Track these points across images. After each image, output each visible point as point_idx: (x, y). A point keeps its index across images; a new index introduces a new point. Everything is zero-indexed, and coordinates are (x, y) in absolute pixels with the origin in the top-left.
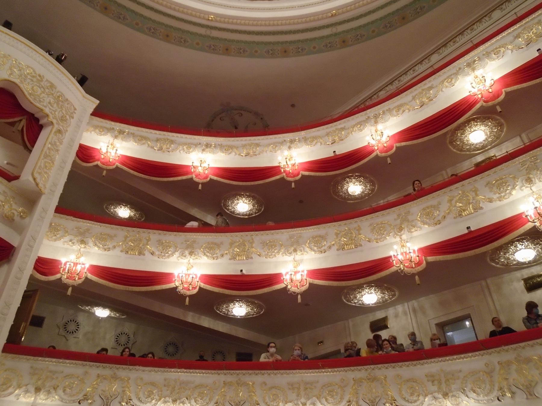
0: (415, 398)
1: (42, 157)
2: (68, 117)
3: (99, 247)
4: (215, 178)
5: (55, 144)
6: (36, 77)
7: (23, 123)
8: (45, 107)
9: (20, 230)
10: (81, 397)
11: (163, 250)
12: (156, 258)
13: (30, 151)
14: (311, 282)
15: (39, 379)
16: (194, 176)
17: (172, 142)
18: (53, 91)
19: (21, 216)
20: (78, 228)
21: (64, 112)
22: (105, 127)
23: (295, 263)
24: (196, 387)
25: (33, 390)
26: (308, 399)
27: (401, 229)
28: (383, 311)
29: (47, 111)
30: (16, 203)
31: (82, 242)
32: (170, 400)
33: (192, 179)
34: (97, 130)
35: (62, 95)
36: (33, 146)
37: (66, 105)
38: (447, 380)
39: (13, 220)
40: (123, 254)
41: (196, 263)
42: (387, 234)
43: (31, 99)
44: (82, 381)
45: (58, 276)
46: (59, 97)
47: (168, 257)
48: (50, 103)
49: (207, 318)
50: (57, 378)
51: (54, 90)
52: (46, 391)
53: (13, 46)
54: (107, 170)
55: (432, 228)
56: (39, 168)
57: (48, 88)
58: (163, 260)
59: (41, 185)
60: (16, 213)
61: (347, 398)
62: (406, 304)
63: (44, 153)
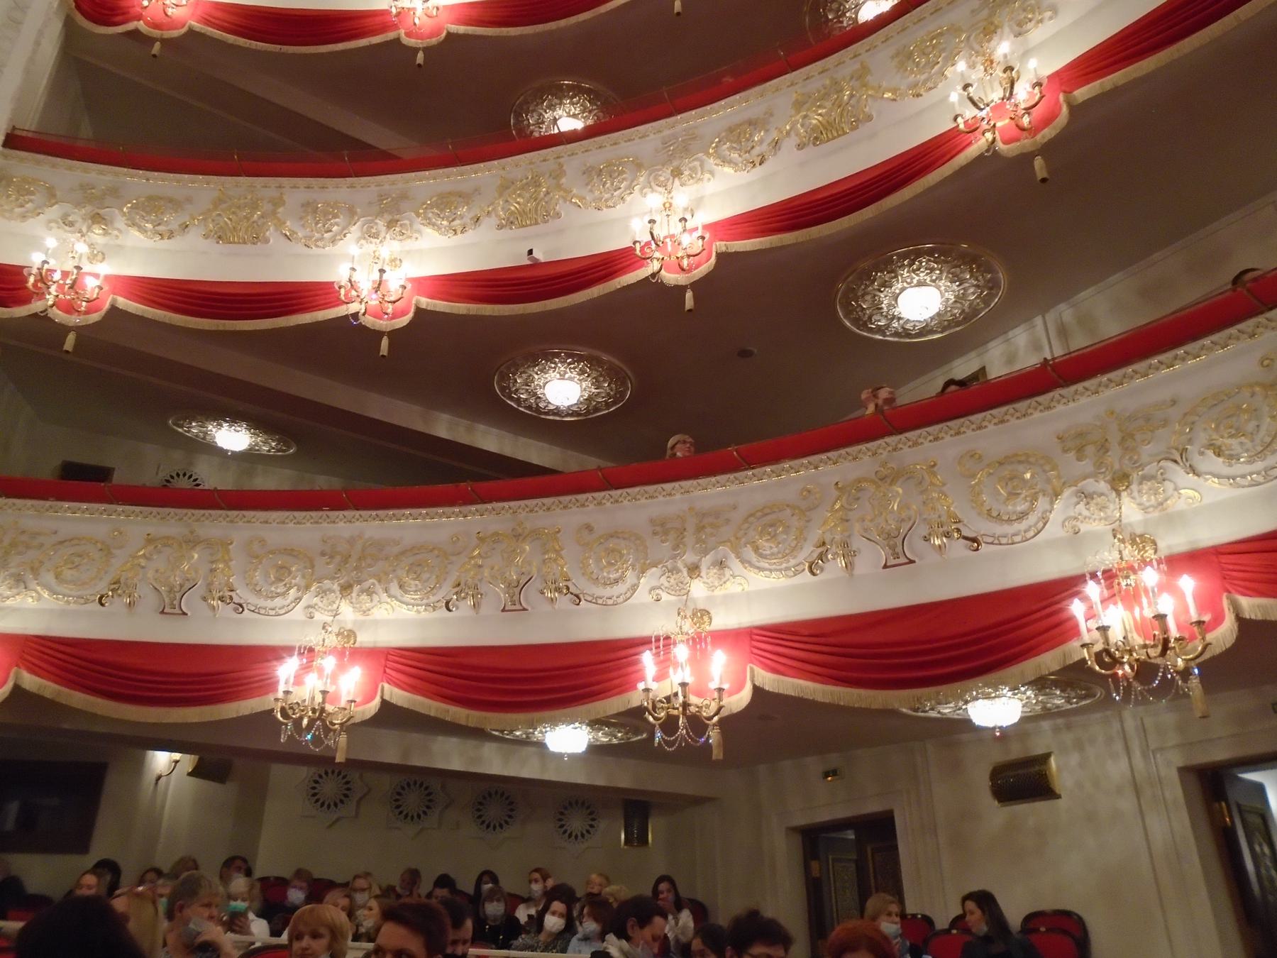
0: (1021, 507)
3: (142, 230)
4: (462, 29)
10: (102, 586)
11: (317, 223)
14: (724, 249)
16: (402, 32)
20: (83, 187)
24: (403, 553)
26: (705, 552)
27: (990, 31)
28: (973, 354)
31: (97, 219)
32: (336, 587)
38: (1127, 438)
40: (210, 246)
41: (409, 252)
44: (107, 550)
47: (333, 241)
49: (494, 430)
50: (42, 545)
52: (12, 575)
54: (164, 42)
58: (320, 251)
61: (816, 534)
62: (1038, 320)
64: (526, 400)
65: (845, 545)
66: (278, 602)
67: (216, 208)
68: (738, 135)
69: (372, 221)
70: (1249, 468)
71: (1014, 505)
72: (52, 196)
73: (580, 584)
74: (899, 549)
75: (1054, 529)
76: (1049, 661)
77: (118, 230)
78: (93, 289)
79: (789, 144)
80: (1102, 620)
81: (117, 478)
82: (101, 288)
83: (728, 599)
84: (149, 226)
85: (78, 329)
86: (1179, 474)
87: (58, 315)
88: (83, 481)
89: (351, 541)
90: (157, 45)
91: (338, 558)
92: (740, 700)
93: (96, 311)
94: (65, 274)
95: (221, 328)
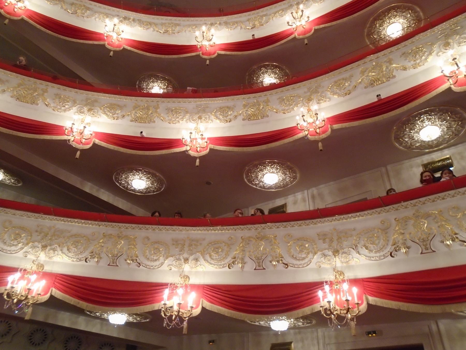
0: (304, 256)
4: (129, 48)
11: (60, 103)
12: (50, 110)
14: (212, 148)
16: (106, 43)
23: (198, 129)
24: (72, 236)
26: (192, 254)
27: (310, 100)
28: (283, 198)
32: (40, 246)
33: (104, 45)
38: (339, 238)
40: (13, 101)
41: (94, 122)
42: (295, 105)
47: (65, 111)
49: (107, 192)
54: (11, 20)
55: (342, 99)
62: (306, 192)
64: (124, 184)
65: (242, 259)
66: (13, 248)
67: (19, 87)
68: (223, 111)
69: (82, 107)
70: (374, 255)
71: (301, 255)
73: (141, 259)
74: (261, 264)
75: (312, 265)
76: (307, 310)
79: (240, 118)
80: (326, 299)
83: (197, 273)
86: (354, 253)
89: (50, 228)
90: (7, 21)
91: (43, 234)
92: (197, 312)
95: (11, 133)
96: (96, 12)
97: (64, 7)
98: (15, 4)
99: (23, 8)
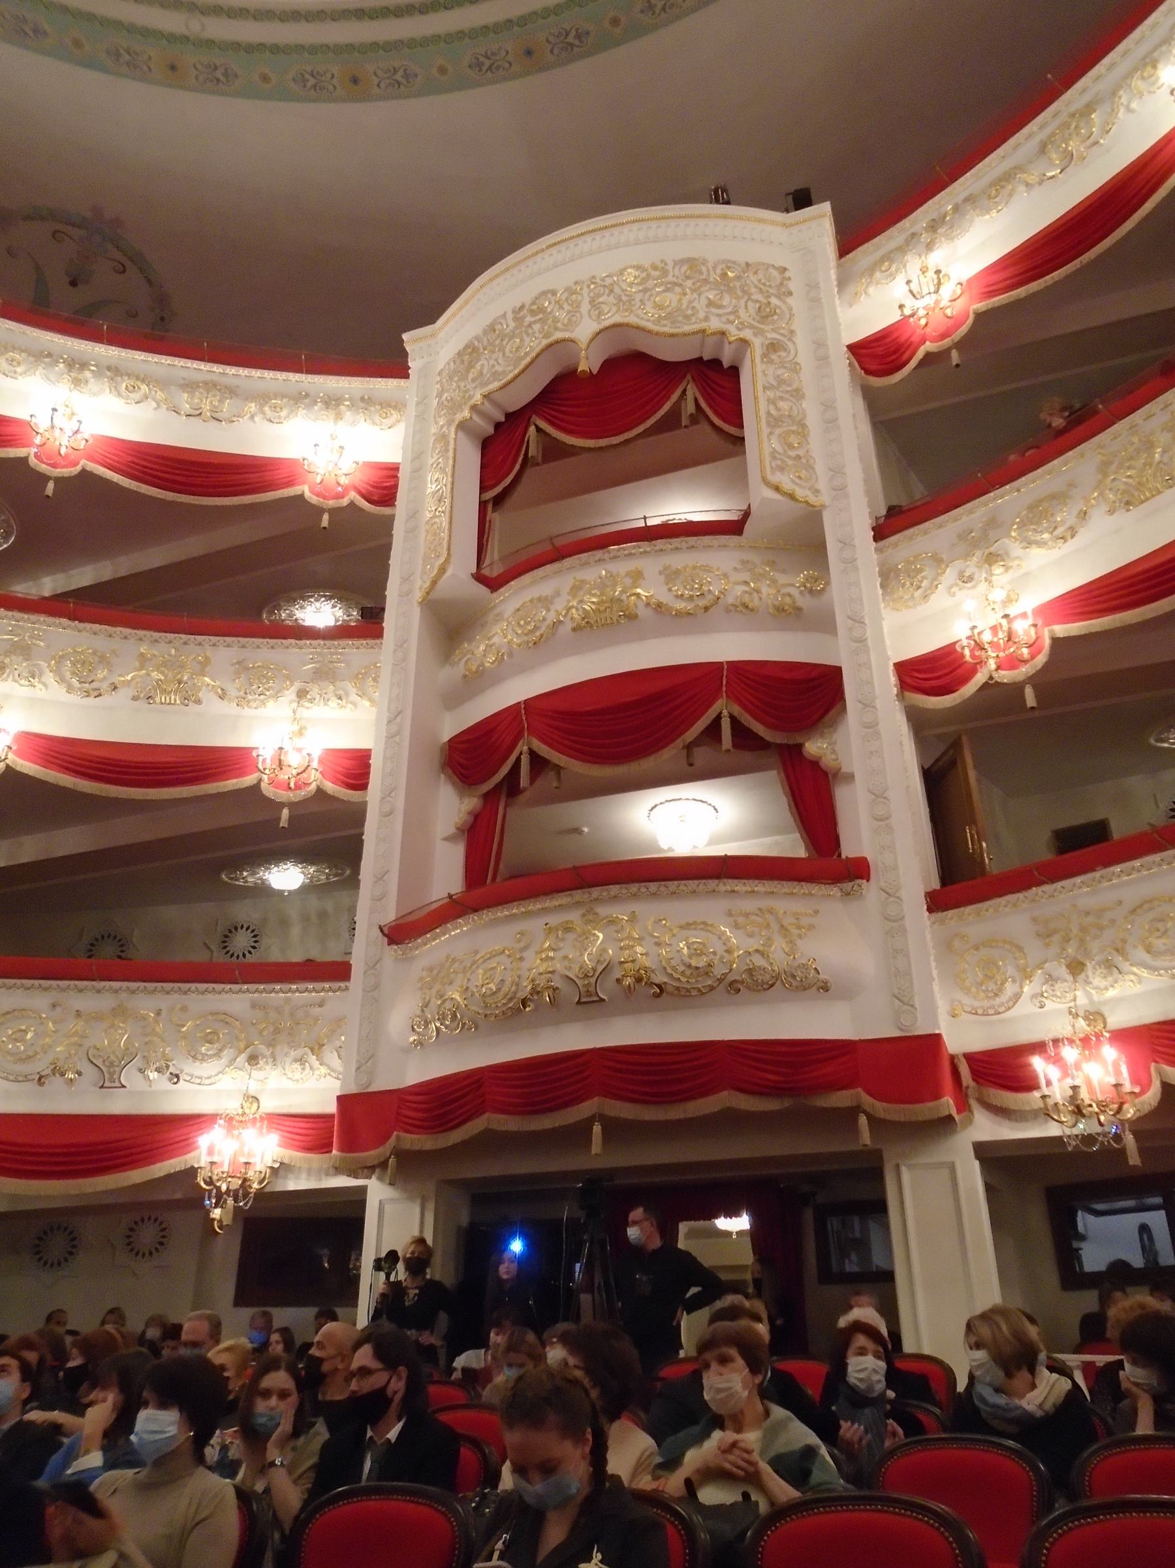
1: (765, 430)
2: (774, 300)
3: (1041, 544)
5: (781, 381)
6: (649, 275)
7: (692, 391)
8: (706, 319)
9: (825, 624)
13: (742, 439)
15: (1067, 940)
17: (1089, 108)
18: (701, 273)
19: (811, 591)
20: (962, 536)
21: (760, 297)
22: (892, 252)
25: (1063, 971)
29: (715, 324)
30: (784, 571)
31: (991, 559)
34: (878, 275)
35: (729, 264)
36: (741, 426)
37: (754, 278)
39: (800, 609)
40: (1122, 518)
43: (669, 329)
45: (980, 678)
46: (724, 275)
48: (710, 303)
50: (1113, 921)
51: (704, 269)
52: (1099, 964)
53: (572, 260)
54: (958, 345)
56: (774, 458)
57: (688, 278)
59: (800, 493)
60: (795, 592)
63: (764, 421)
67: (1105, 475)
72: (938, 562)
77: (1017, 558)
78: (1026, 633)
81: (1118, 830)
82: (1035, 626)
84: (1046, 536)
85: (1032, 679)
87: (1005, 676)
88: (1084, 847)
90: (954, 354)
93: (1039, 652)
94: (994, 629)
96: (1114, 93)
97: (1033, 178)
98: (937, 302)
99: (959, 292)
